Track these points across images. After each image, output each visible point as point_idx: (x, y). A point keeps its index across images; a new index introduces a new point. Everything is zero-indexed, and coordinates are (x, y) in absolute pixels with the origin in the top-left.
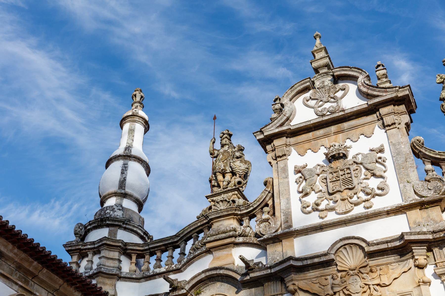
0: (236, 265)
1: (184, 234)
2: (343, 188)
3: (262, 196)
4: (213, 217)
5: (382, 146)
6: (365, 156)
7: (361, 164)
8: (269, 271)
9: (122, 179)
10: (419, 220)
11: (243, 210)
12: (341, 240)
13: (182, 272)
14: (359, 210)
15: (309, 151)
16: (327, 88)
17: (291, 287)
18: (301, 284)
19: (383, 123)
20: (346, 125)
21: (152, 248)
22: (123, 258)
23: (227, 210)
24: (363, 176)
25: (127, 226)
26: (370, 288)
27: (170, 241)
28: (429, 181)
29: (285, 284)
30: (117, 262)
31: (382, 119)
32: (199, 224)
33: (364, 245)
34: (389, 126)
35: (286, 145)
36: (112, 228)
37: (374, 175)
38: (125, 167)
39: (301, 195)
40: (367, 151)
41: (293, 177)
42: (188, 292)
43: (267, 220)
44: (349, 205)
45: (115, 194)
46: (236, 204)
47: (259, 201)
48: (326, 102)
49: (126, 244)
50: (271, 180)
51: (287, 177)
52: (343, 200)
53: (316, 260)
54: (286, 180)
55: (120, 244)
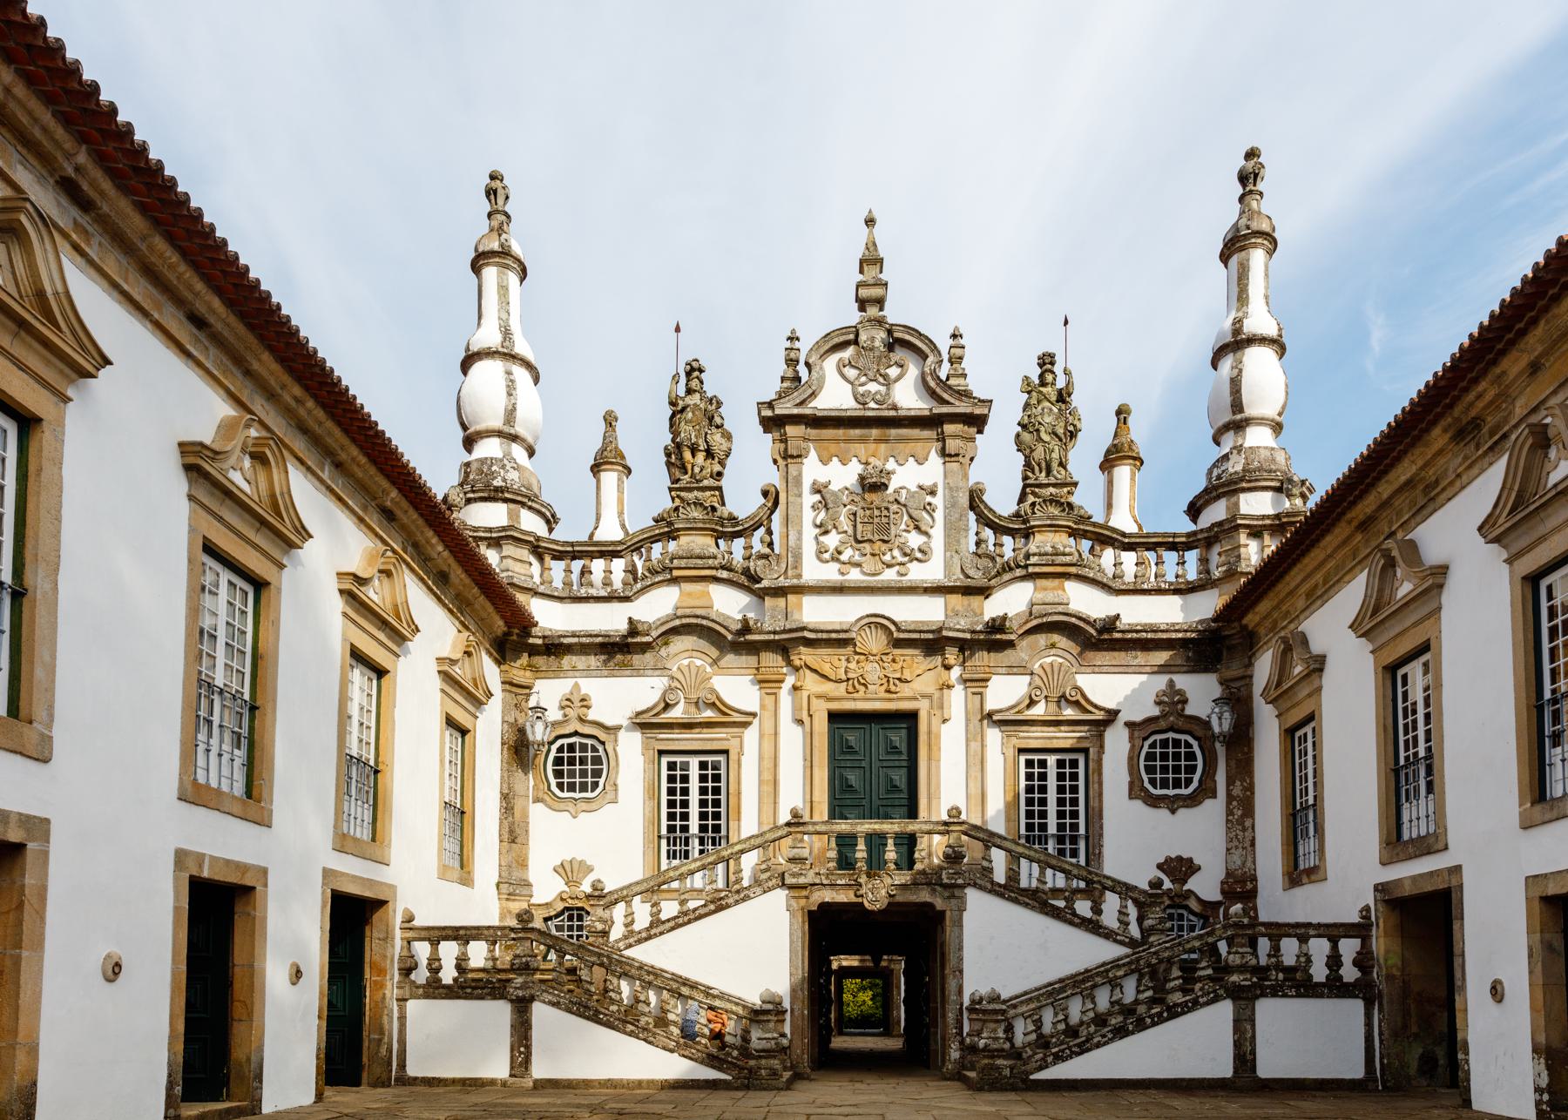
0: (715, 609)
1: (633, 542)
2: (877, 537)
3: (758, 514)
4: (681, 526)
5: (935, 485)
6: (911, 495)
7: (905, 506)
8: (772, 637)
9: (510, 407)
10: (959, 608)
11: (726, 527)
12: (868, 616)
13: (632, 601)
14: (890, 575)
15: (835, 459)
16: (877, 354)
17: (797, 663)
18: (810, 660)
19: (943, 448)
20: (893, 432)
21: (578, 551)
22: (532, 559)
23: (703, 521)
24: (903, 527)
25: (534, 505)
26: (888, 681)
27: (610, 549)
28: (979, 556)
29: (789, 657)
30: (528, 566)
31: (944, 441)
32: (657, 532)
33: (893, 628)
34: (950, 456)
35: (805, 439)
36: (512, 506)
37: (917, 528)
38: (512, 381)
39: (817, 531)
40: (914, 489)
41: (809, 499)
42: (654, 640)
43: (766, 557)
44: (880, 565)
45: (500, 434)
46: (718, 514)
47: (752, 519)
48: (871, 380)
49: (538, 539)
50: (773, 489)
51: (800, 495)
52: (873, 555)
53: (834, 636)
54: (798, 499)
55: (532, 539)
